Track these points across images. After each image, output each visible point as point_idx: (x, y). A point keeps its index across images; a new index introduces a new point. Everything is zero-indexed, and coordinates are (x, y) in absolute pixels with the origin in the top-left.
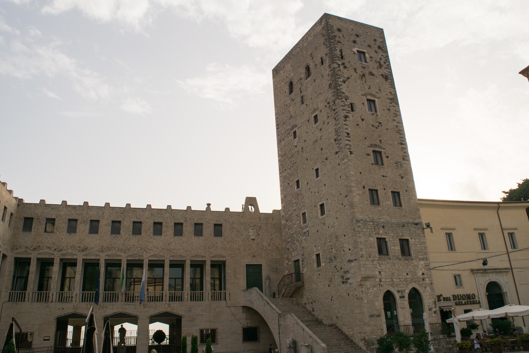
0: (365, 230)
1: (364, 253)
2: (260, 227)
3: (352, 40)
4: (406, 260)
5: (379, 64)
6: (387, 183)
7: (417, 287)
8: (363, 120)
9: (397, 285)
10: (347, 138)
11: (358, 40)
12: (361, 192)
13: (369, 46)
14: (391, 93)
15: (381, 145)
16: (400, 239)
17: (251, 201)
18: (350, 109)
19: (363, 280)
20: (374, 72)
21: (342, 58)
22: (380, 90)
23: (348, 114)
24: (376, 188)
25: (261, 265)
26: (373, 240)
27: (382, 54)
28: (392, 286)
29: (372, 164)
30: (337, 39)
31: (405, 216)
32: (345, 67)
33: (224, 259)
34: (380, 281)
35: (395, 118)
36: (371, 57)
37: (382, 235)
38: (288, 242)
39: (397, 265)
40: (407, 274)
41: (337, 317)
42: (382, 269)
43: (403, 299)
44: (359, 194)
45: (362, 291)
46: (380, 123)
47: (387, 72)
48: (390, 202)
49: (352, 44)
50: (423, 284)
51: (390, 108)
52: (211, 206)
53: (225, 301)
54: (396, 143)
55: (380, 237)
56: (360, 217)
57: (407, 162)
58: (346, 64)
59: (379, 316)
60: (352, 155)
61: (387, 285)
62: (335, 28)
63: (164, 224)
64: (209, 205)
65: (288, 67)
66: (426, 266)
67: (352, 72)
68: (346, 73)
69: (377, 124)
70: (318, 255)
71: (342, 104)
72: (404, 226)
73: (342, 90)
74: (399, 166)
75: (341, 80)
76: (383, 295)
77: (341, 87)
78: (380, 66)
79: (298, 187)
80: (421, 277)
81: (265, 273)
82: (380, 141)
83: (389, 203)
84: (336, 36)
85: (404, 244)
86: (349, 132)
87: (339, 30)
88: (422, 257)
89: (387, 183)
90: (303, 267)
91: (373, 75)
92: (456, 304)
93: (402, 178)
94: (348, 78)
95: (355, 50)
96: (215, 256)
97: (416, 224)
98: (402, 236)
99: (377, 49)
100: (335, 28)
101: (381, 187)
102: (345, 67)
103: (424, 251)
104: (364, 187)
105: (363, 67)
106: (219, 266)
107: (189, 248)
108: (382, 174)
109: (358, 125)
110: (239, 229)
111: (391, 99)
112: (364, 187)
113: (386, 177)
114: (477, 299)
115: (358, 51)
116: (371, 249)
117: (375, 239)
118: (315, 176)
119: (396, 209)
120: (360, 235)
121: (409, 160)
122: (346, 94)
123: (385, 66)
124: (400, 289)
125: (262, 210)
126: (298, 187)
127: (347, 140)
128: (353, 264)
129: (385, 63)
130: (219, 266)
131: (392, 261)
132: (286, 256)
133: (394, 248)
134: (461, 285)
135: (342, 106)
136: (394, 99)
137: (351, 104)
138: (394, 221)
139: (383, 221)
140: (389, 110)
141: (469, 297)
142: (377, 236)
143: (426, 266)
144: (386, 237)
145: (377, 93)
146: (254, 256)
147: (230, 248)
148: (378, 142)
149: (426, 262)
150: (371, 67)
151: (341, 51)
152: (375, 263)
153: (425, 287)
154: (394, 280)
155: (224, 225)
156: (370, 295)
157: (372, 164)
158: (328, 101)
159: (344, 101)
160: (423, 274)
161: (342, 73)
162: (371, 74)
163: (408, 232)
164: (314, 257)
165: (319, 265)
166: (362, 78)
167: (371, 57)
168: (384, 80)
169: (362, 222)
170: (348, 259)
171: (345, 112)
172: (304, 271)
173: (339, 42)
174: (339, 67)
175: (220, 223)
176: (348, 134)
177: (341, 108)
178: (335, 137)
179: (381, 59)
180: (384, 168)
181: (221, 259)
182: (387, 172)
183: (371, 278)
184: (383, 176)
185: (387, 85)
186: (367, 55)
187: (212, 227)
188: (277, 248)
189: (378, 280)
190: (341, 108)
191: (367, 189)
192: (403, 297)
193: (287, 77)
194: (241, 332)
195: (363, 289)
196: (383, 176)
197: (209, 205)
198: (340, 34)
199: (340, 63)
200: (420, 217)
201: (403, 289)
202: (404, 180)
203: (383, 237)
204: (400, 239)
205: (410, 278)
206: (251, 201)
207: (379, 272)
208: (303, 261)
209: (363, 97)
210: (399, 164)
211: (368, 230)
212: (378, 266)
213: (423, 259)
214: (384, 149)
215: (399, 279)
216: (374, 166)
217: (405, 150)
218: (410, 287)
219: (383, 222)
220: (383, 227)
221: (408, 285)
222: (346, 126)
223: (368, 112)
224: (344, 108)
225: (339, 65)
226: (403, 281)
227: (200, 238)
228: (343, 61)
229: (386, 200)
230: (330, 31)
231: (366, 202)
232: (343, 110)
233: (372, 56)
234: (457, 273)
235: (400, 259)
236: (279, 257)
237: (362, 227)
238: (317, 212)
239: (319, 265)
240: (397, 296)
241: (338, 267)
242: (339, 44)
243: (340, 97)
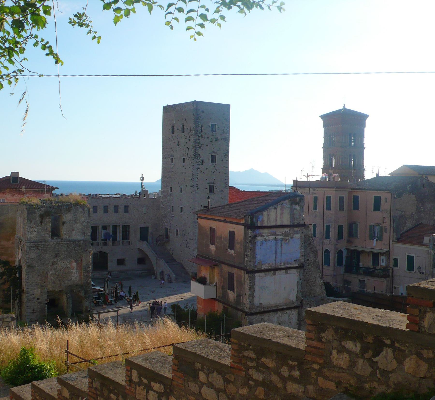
18: (201, 164)
35: (225, 165)
38: (164, 217)
63: (98, 207)
70: (177, 230)
79: (171, 191)
81: (150, 230)
102: (203, 137)
106: (126, 229)
107: (112, 219)
126: (171, 191)
128: (191, 241)
130: (126, 229)
137: (202, 161)
164: (176, 231)
165: (177, 234)
172: (170, 235)
176: (198, 178)
186: (217, 127)
187: (123, 208)
194: (137, 260)
199: (200, 135)
239: (177, 234)
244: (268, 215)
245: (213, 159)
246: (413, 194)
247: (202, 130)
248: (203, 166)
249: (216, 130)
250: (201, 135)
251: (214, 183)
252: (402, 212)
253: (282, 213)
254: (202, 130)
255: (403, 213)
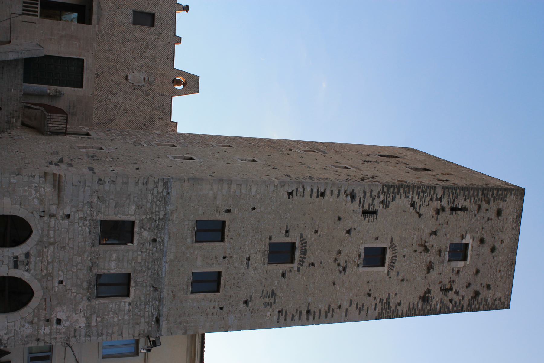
0: (150, 197)
1: (107, 187)
2: (148, 94)
3: (485, 236)
4: (89, 283)
5: (448, 287)
6: (236, 264)
7: (34, 303)
8: (348, 232)
9: (40, 254)
10: (315, 190)
11: (486, 249)
12: (219, 202)
13: (478, 272)
14: (399, 304)
15: (306, 264)
16: (129, 275)
17: (191, 84)
18: (366, 207)
19: (54, 180)
20: (434, 274)
21: (453, 209)
22: (403, 280)
23: (357, 200)
24: (226, 239)
25: (82, 87)
26: (128, 213)
27: (466, 299)
28: (40, 242)
29: (270, 238)
30: (484, 205)
31: (174, 296)
33: (94, 21)
34: (52, 216)
35: (354, 305)
36: (458, 272)
37: (140, 233)
39: (79, 259)
40: (61, 282)
42: (73, 223)
43: (11, 265)
45: (33, 176)
46: (344, 269)
47: (434, 302)
48: (201, 267)
49: (478, 236)
50: (39, 320)
51: (371, 298)
52: (184, 12)
53: (21, 12)
54: (310, 299)
55: (136, 229)
56: (174, 191)
57: (275, 318)
58: (442, 214)
60: (286, 196)
61: (42, 231)
62: (502, 205)
64: (187, 8)
65: (422, 158)
66: (75, 331)
67: (432, 225)
68: (428, 211)
69: (343, 264)
71: (375, 193)
72: (156, 289)
73: (398, 197)
74: (267, 300)
75: (416, 198)
76: (22, 216)
77: (403, 195)
78: (445, 290)
80: (54, 315)
81: (67, 91)
82: (313, 264)
83: (199, 263)
84: (488, 202)
85: (120, 285)
86: (326, 198)
87: (499, 213)
88: (94, 323)
89: (236, 264)
91: (429, 272)
93: (246, 302)
94: (420, 215)
95: (468, 240)
96: (99, 6)
97: (158, 321)
98: (135, 281)
99: (473, 287)
100: (502, 205)
101: (229, 251)
102: (438, 212)
103: (105, 332)
104: (228, 211)
105: (440, 251)
108: (253, 257)
109: (340, 219)
110: (145, 55)
111: (388, 303)
112: (228, 211)
113: (248, 264)
115: (467, 245)
116: (113, 204)
117: (132, 218)
119: (187, 279)
120: (140, 184)
121: (278, 324)
122: (392, 205)
123: (446, 301)
124: (32, 259)
125: (176, 100)
127: (312, 190)
129: (451, 301)
131: (88, 248)
135: (371, 191)
136: (387, 311)
137: (375, 213)
138: (166, 267)
139: (166, 242)
140: (369, 295)
142: (137, 222)
143: (75, 331)
144: (135, 242)
145: (398, 273)
146: (97, 75)
147: (113, 35)
148: (311, 258)
149: (83, 333)
150: (441, 268)
151: (464, 209)
152: (87, 209)
153: (31, 323)
154: (52, 248)
155: (152, 29)
156: (25, 191)
157: (270, 238)
159: (379, 197)
160: (59, 321)
161: (426, 203)
162: (430, 267)
163: (143, 298)
166: (420, 245)
167: (458, 272)
168: (421, 293)
169: (165, 193)
171: (362, 196)
173: (479, 207)
174: (437, 199)
175: (156, 24)
177: (368, 190)
179: (457, 293)
180: (264, 263)
181: (95, 16)
182: (256, 269)
183: (59, 196)
184: (248, 259)
185: (412, 297)
186: (461, 264)
187: (149, 10)
188: (111, 120)
189: (53, 209)
190: (368, 190)
192: (16, 266)
195: (37, 179)
196: (248, 259)
197: (187, 8)
198: (492, 214)
199: (444, 203)
200: (170, 332)
201: (32, 266)
202: (242, 306)
203: (136, 237)
204: (129, 275)
205: (53, 287)
206: (191, 84)
207: (68, 216)
209: (389, 240)
210: (272, 300)
211: (149, 205)
212: (81, 215)
213: (89, 326)
214: (298, 269)
215: (53, 261)
216: (268, 241)
218: (35, 286)
219: (163, 241)
220: (154, 240)
221: (40, 280)
222: (336, 192)
223: (363, 246)
224: (368, 195)
225: (440, 200)
226: (47, 269)
228: (447, 209)
229: (206, 258)
230: (495, 192)
231: (200, 212)
232: (365, 193)
233: (461, 274)
235: (91, 270)
236: (95, 121)
237: (156, 191)
240: (19, 251)
242: (476, 207)
243: (385, 190)
248: (360, 216)
249: (453, 264)
251: (302, 261)
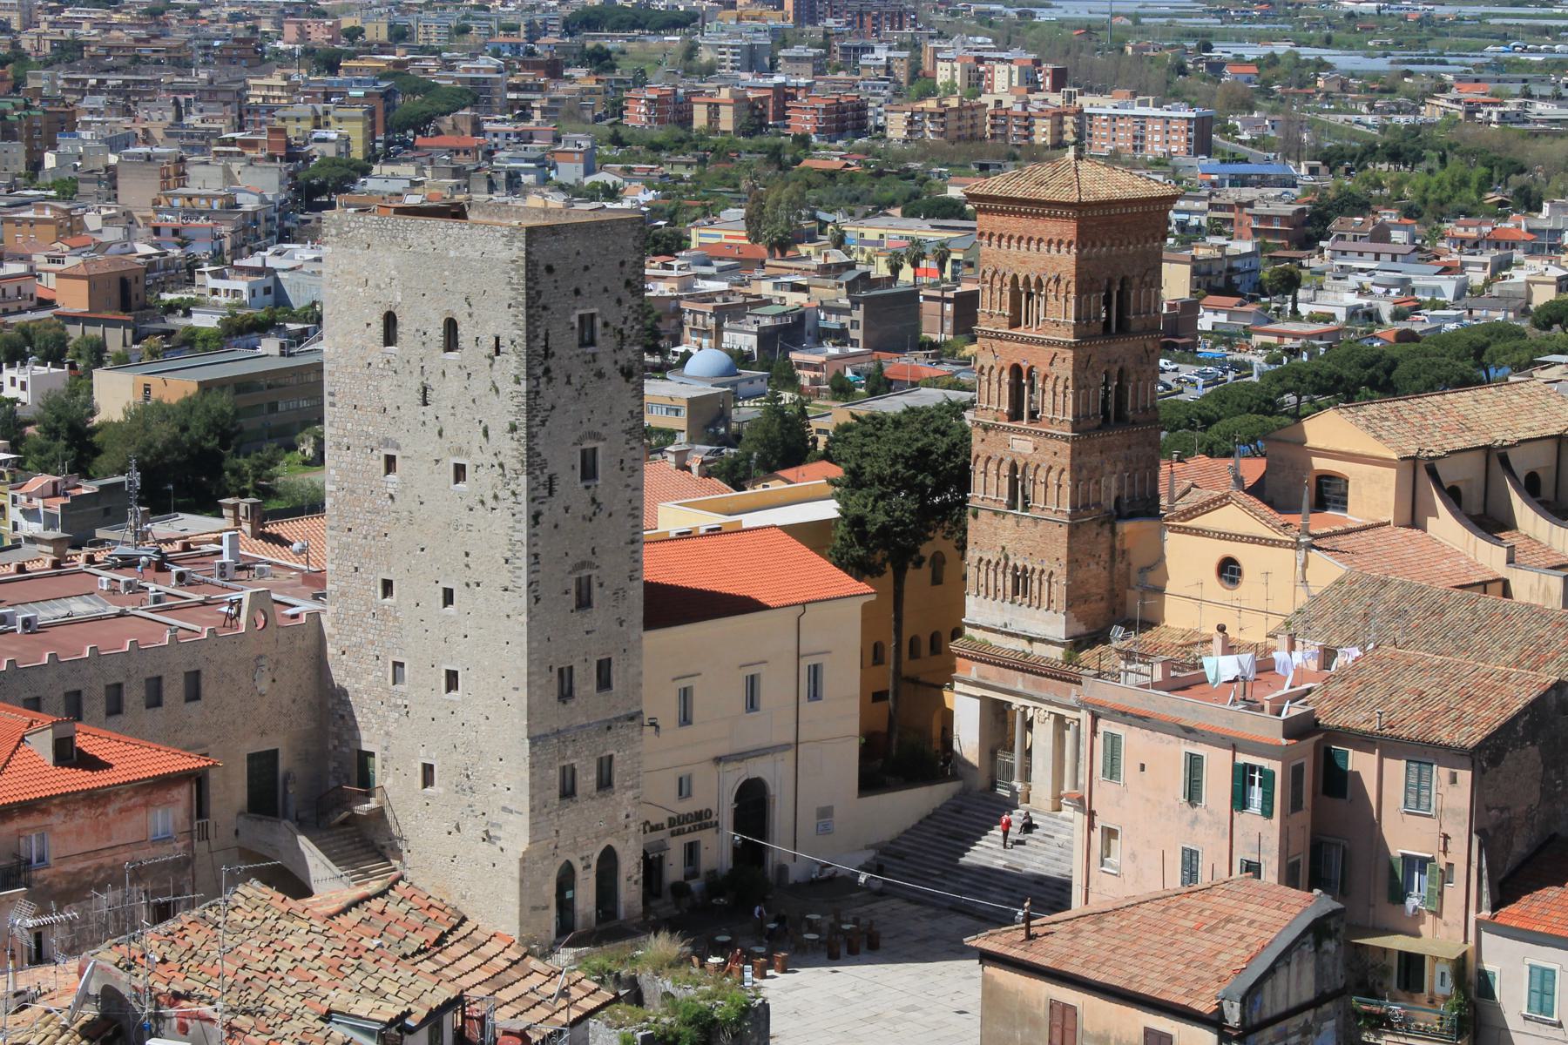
2: (278, 662)
14: (631, 412)
18: (546, 493)
26: (554, 774)
32: (550, 380)
35: (630, 481)
41: (464, 897)
44: (540, 687)
59: (547, 908)
81: (283, 766)
90: (387, 775)
92: (673, 834)
114: (714, 819)
118: (441, 601)
128: (511, 817)
132: (335, 729)
133: (587, 780)
134: (689, 795)
141: (699, 815)
148: (588, 557)
155: (204, 673)
158: (501, 458)
170: (502, 803)
176: (536, 556)
178: (508, 555)
186: (598, 322)
191: (555, 670)
193: (378, 286)
208: (385, 760)
213: (632, 787)
217: (636, 556)
227: (159, 710)
234: (683, 771)
238: (437, 681)
240: (578, 866)
241: (479, 809)
244: (1273, 987)
245: (589, 470)
246: (1533, 744)
247: (546, 348)
249: (598, 336)
250: (547, 371)
251: (591, 565)
252: (1502, 810)
253: (1299, 974)
254: (546, 348)
255: (1506, 815)
